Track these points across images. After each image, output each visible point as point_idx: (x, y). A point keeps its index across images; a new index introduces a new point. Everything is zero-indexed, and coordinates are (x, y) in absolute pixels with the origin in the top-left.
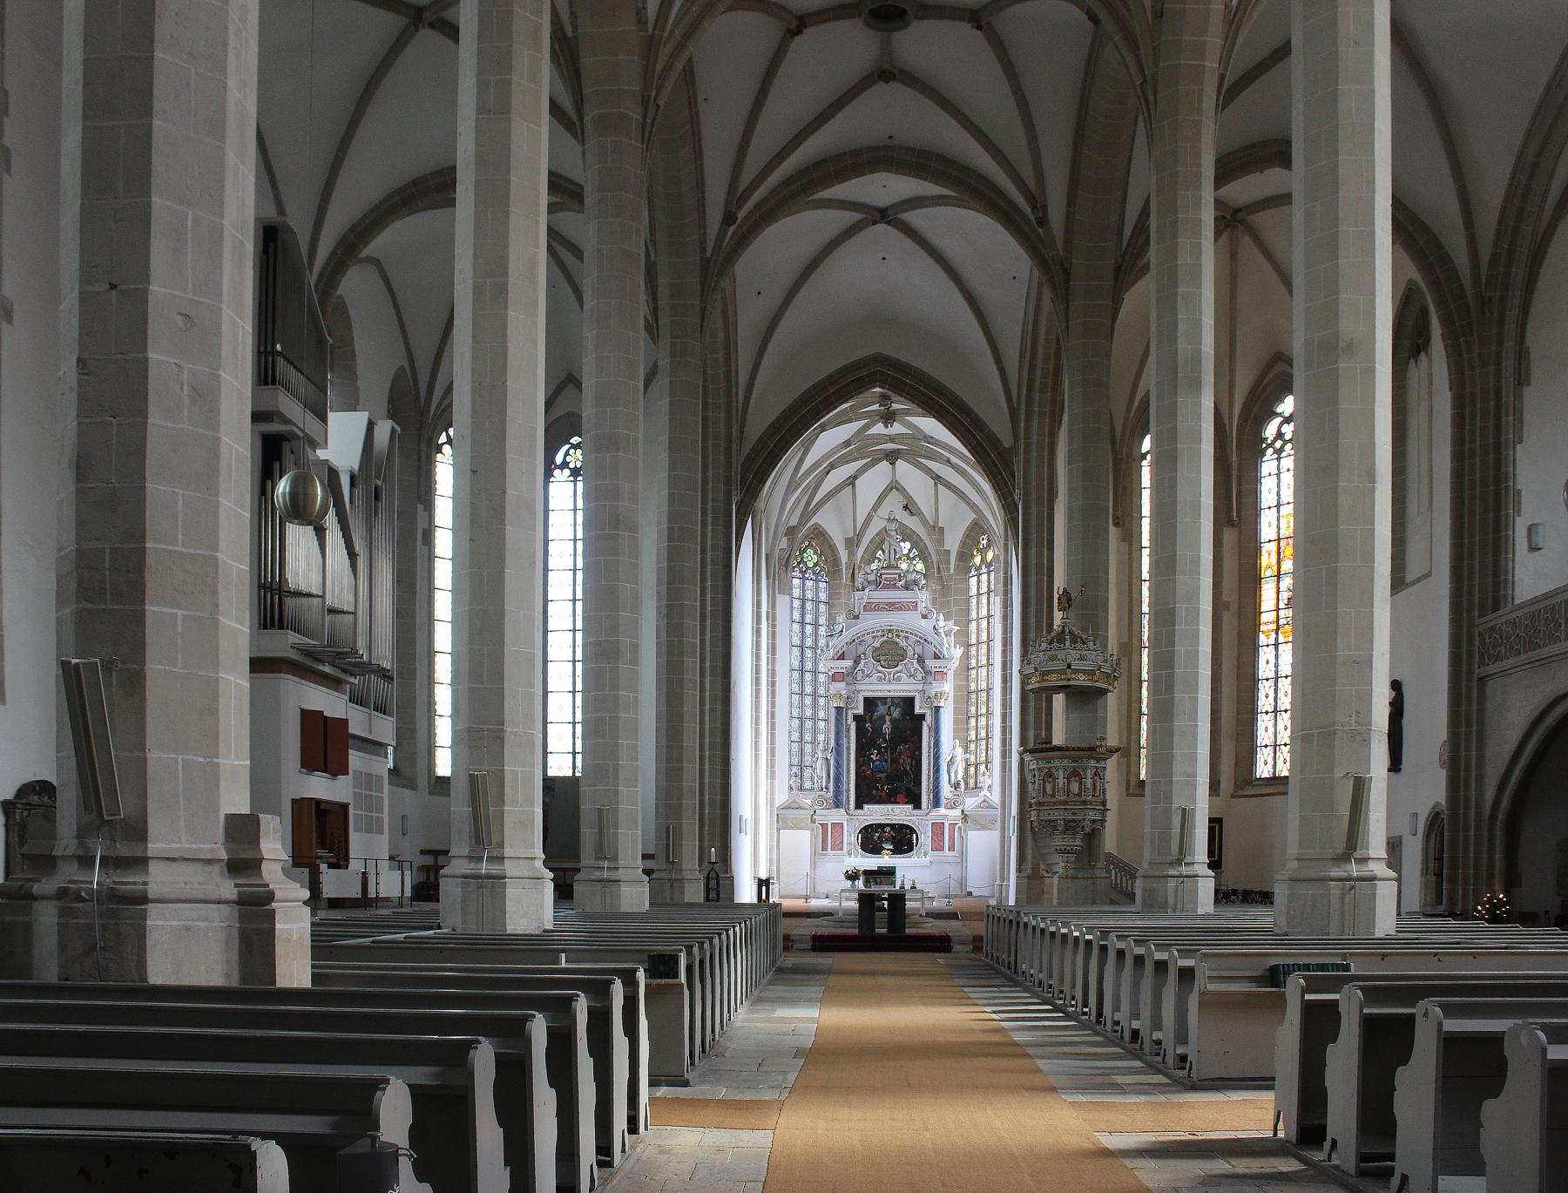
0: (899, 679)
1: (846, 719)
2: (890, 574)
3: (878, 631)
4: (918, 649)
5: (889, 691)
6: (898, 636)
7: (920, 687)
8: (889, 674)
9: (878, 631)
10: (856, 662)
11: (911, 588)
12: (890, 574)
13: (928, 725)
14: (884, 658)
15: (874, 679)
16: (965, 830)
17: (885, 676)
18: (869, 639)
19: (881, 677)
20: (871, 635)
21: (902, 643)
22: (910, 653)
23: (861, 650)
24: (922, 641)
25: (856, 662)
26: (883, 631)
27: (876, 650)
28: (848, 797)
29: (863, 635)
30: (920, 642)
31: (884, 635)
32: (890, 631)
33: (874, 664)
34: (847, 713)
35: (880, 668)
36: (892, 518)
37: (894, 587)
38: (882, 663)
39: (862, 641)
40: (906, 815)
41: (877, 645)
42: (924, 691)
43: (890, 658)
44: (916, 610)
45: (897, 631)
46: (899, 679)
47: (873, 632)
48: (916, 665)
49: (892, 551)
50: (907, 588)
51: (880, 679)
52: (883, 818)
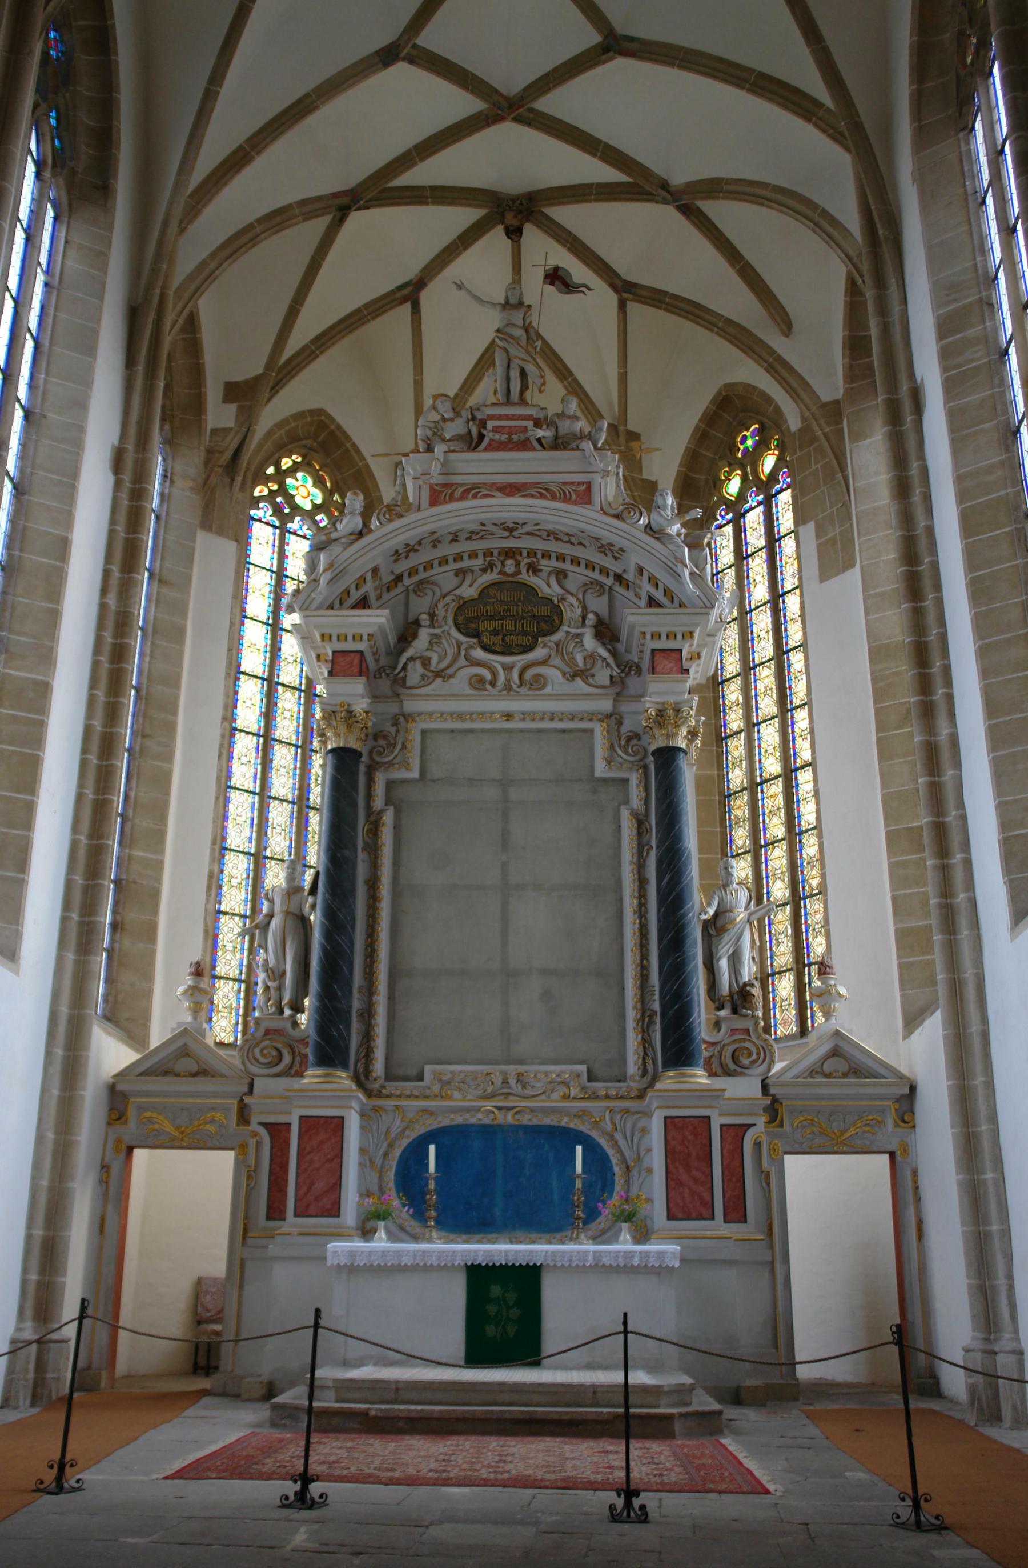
0: (539, 682)
1: (369, 796)
2: (508, 417)
3: (474, 555)
4: (598, 604)
5: (508, 716)
6: (533, 568)
7: (606, 705)
8: (508, 668)
9: (474, 555)
10: (407, 634)
11: (574, 445)
12: (508, 417)
13: (635, 814)
14: (490, 625)
15: (460, 682)
16: (772, 1149)
17: (494, 674)
18: (445, 578)
19: (481, 680)
20: (453, 566)
21: (548, 588)
22: (572, 610)
23: (420, 605)
24: (609, 581)
25: (407, 634)
26: (488, 553)
27: (463, 605)
28: (367, 1037)
29: (428, 566)
30: (601, 585)
31: (491, 566)
32: (510, 553)
33: (459, 645)
34: (370, 781)
35: (479, 654)
36: (513, 300)
37: (524, 445)
38: (486, 639)
39: (421, 582)
40: (566, 1097)
41: (469, 592)
42: (614, 719)
43: (509, 625)
44: (589, 502)
45: (532, 553)
46: (539, 682)
47: (459, 557)
48: (590, 642)
49: (515, 374)
50: (559, 443)
51: (478, 684)
52: (489, 1105)
